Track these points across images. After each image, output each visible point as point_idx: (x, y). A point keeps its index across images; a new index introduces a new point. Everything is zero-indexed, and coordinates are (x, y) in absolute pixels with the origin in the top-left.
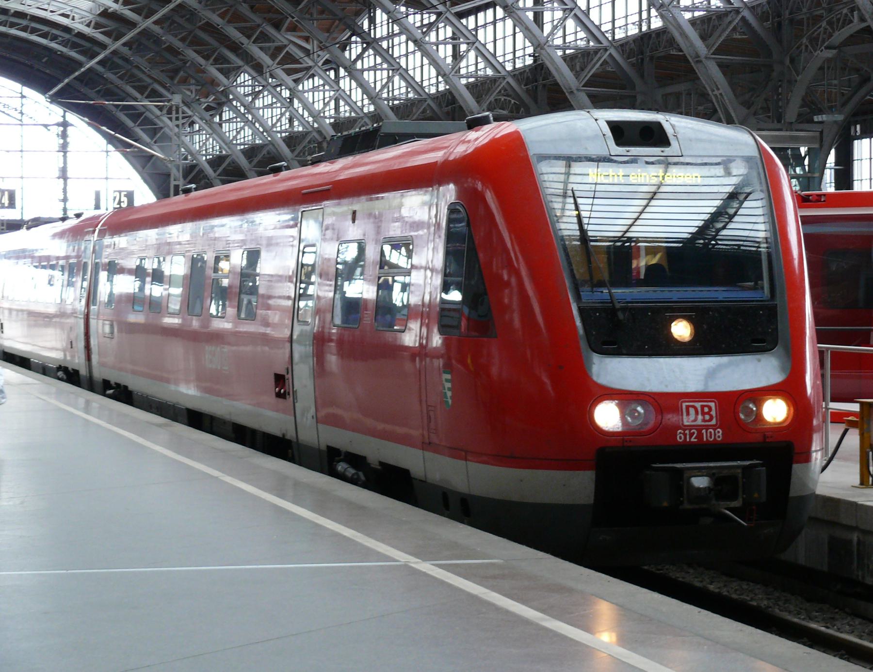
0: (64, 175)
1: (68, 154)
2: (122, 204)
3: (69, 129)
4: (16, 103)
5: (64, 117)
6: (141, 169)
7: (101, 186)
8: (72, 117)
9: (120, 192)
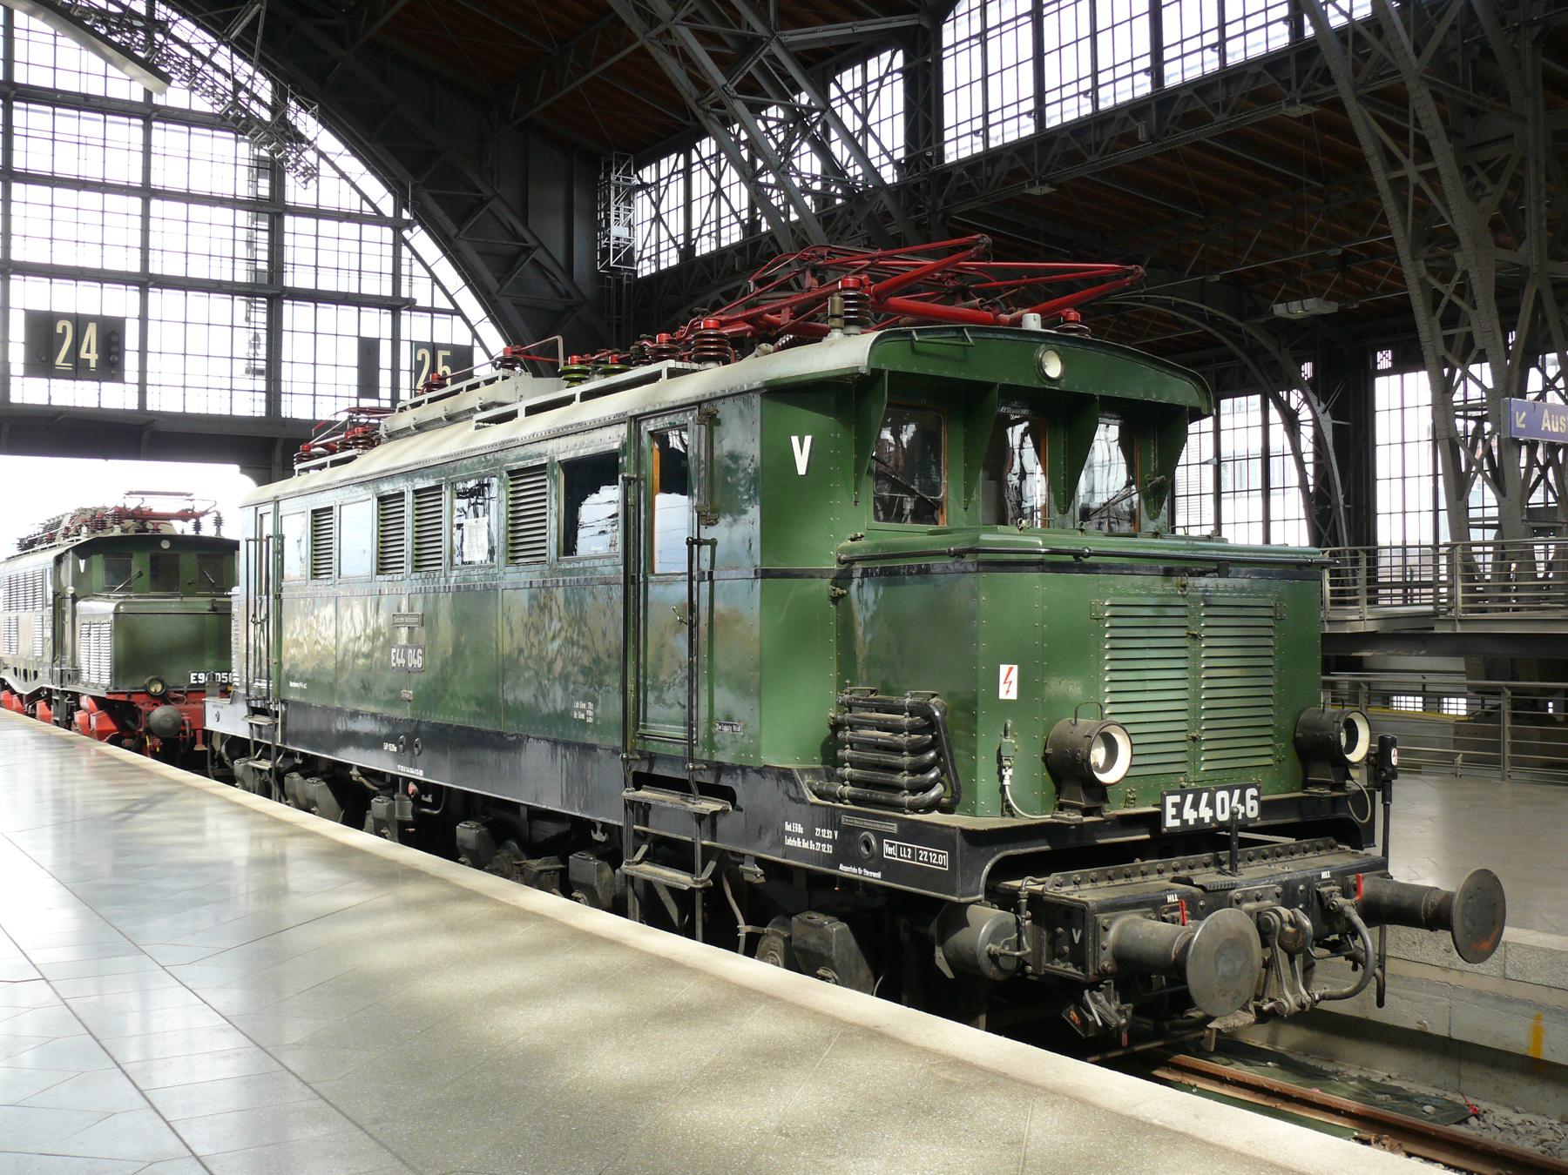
5: (277, 108)
6: (493, 284)
9: (433, 348)
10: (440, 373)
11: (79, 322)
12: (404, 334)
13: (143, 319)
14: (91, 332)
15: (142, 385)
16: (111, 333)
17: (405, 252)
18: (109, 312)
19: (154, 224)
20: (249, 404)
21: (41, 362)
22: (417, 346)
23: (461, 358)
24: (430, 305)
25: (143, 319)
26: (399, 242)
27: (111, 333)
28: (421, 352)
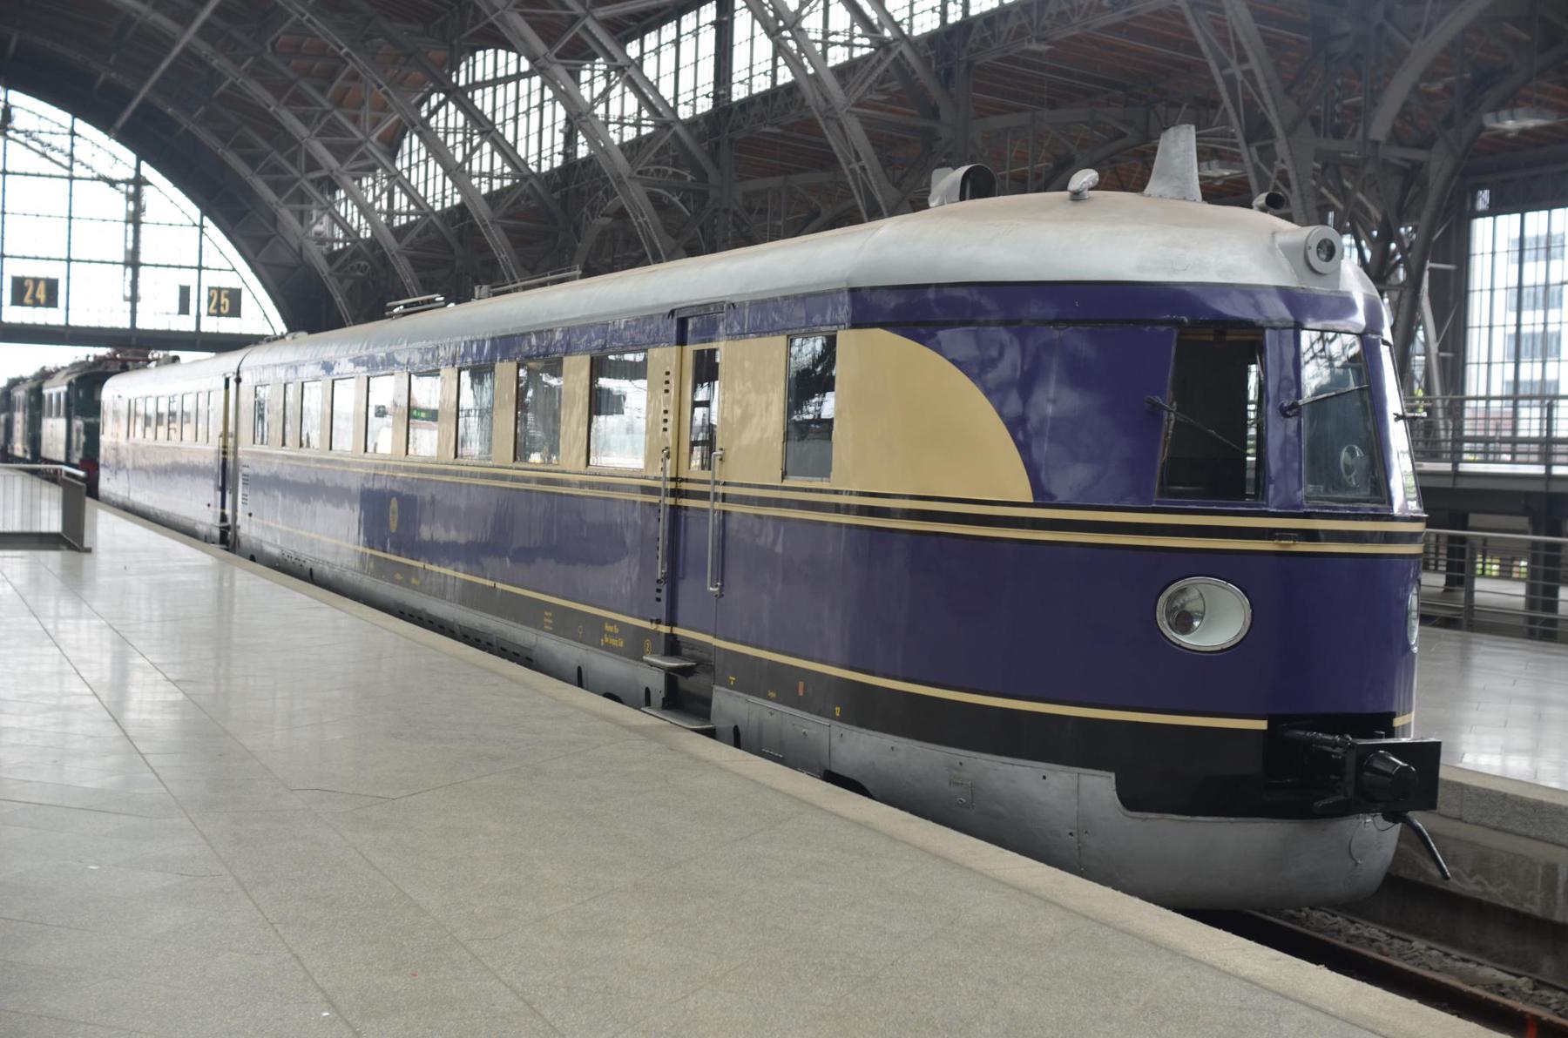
0: (133, 261)
1: (143, 228)
2: (222, 308)
3: (146, 189)
4: (63, 142)
5: (138, 169)
6: (251, 256)
7: (190, 278)
8: (148, 171)
9: (219, 290)
10: (222, 302)
11: (36, 281)
14: (42, 286)
15: (67, 309)
16: (52, 286)
17: (204, 237)
18: (52, 276)
21: (18, 300)
22: (210, 289)
23: (235, 296)
26: (202, 232)
27: (52, 286)
28: (212, 291)
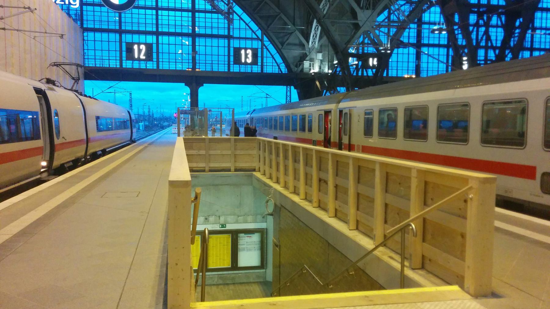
12: (231, 45)
13: (158, 43)
15: (158, 62)
19: (160, 17)
20: (186, 67)
24: (239, 36)
25: (158, 43)
